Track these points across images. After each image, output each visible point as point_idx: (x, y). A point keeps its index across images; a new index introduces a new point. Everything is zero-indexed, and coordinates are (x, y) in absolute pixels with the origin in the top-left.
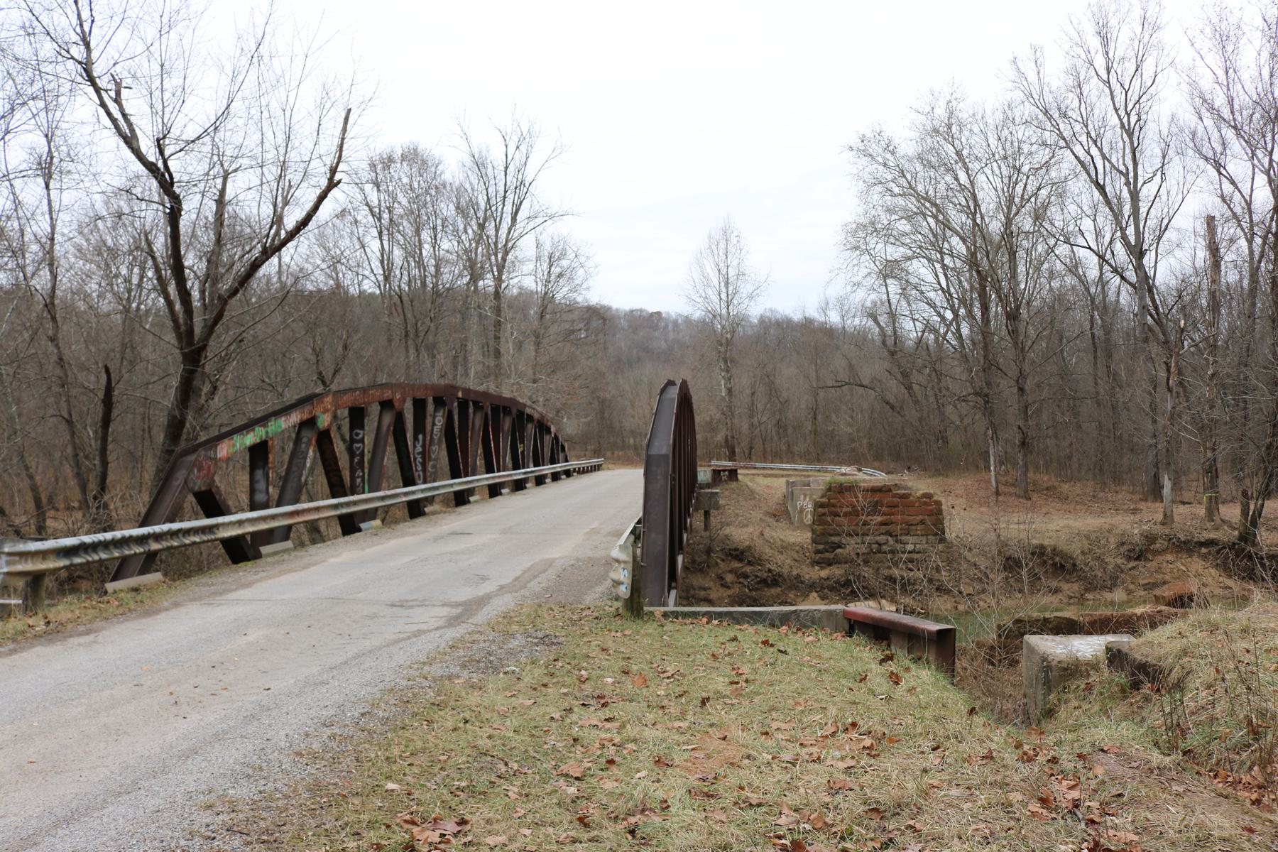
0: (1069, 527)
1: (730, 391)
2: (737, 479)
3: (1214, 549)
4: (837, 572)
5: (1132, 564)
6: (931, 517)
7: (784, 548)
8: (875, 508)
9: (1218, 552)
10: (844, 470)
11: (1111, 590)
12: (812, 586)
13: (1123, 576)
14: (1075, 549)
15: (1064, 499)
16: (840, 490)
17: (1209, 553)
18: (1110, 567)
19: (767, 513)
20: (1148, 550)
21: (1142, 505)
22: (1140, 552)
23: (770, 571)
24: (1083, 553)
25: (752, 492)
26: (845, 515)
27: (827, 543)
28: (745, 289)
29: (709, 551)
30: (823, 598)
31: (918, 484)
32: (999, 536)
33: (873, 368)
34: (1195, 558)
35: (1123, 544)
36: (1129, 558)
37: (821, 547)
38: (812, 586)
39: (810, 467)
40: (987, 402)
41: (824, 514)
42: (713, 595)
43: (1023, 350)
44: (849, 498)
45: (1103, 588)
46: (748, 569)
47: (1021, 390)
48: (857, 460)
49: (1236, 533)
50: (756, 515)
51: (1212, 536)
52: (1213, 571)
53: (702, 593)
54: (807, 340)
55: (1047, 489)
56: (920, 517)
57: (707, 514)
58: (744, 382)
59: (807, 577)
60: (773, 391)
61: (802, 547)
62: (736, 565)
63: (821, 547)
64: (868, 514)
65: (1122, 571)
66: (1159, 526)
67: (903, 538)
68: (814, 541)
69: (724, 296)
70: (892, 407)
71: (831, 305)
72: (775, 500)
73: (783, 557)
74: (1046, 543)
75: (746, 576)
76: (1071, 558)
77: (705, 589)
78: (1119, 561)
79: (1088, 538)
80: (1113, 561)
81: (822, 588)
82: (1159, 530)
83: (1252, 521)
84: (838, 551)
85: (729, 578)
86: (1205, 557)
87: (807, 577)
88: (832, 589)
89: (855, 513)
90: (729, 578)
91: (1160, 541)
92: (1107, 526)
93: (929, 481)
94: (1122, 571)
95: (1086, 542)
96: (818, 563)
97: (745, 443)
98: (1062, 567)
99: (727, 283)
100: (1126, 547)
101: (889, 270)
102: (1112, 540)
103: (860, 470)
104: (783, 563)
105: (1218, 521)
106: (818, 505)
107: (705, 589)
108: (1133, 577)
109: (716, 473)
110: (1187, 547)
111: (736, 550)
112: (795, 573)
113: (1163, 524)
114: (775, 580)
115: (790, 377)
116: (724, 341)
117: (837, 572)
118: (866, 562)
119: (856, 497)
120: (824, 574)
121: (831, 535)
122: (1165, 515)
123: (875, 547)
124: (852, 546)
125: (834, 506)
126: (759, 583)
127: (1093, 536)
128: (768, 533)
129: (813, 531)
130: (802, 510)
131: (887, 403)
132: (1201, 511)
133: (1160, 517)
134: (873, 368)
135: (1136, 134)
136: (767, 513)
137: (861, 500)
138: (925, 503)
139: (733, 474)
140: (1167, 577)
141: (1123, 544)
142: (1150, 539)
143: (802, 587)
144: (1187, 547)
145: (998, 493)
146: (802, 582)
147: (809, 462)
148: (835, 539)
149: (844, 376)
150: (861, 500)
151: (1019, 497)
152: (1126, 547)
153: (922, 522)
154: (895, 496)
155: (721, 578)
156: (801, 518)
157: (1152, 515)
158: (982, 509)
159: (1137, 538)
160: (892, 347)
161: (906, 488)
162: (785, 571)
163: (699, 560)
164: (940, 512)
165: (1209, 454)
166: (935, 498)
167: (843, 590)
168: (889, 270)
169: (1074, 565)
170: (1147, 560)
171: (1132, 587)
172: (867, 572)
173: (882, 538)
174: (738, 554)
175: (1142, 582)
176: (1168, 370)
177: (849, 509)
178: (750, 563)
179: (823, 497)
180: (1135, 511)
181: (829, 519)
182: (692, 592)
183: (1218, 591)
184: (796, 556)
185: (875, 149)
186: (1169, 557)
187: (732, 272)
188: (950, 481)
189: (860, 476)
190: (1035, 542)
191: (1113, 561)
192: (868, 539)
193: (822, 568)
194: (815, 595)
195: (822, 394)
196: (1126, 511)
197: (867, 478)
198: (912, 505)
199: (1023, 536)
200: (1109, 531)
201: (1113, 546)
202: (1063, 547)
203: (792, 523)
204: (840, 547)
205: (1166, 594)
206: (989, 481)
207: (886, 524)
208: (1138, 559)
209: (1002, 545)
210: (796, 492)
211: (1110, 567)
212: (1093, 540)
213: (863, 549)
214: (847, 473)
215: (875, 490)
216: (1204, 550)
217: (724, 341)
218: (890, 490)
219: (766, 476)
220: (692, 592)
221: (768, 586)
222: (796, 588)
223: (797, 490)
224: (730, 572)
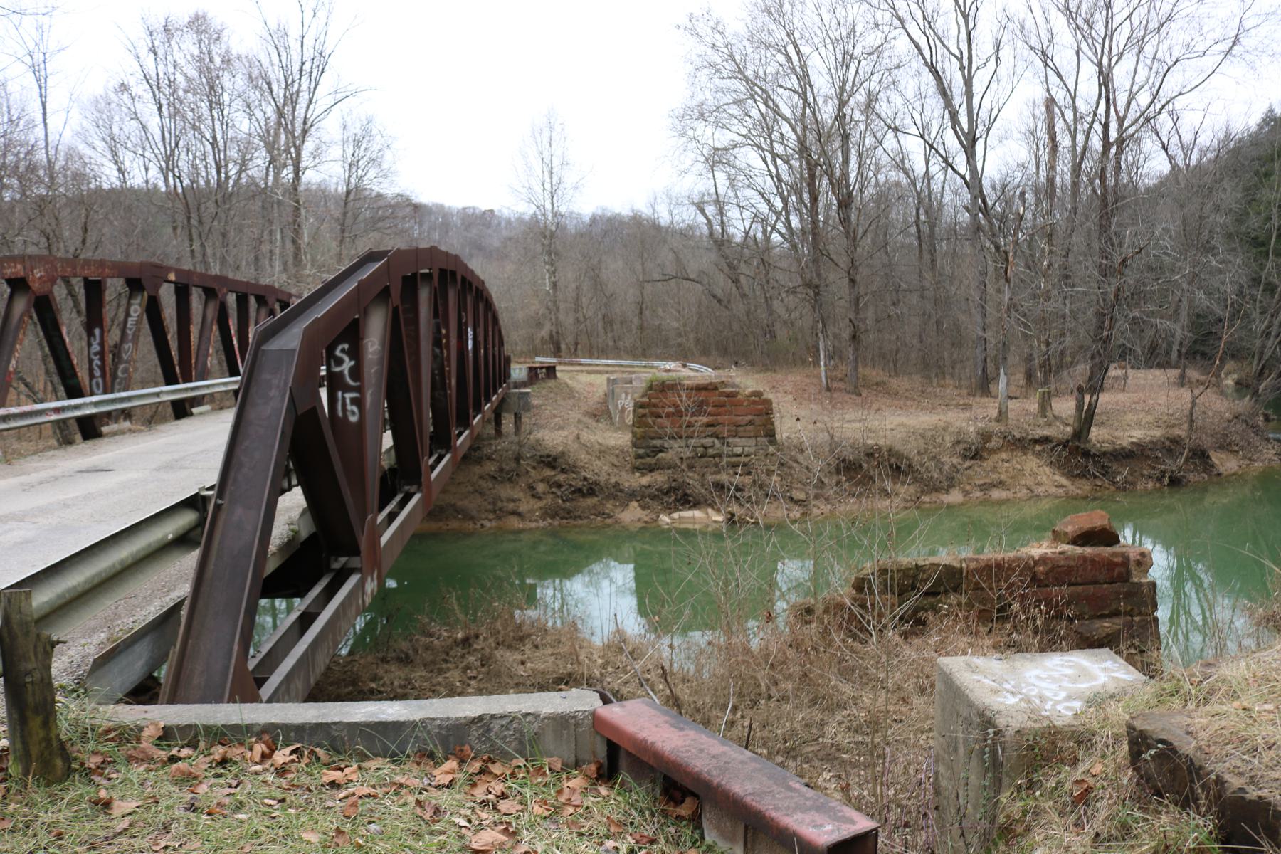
0: (902, 425)
1: (554, 285)
2: (555, 377)
3: (1050, 446)
4: (659, 478)
5: (968, 464)
6: (761, 416)
7: (603, 452)
8: (700, 408)
9: (1052, 449)
10: (670, 365)
11: (947, 492)
12: (632, 495)
13: (959, 476)
14: (911, 449)
15: (894, 394)
16: (662, 388)
17: (1044, 450)
18: (946, 467)
19: (586, 413)
20: (984, 449)
21: (970, 400)
22: (976, 453)
23: (585, 479)
24: (919, 453)
25: (571, 390)
26: (668, 415)
27: (648, 447)
28: (569, 178)
29: (517, 459)
30: (644, 508)
31: (746, 381)
32: (832, 437)
33: (702, 262)
34: (1030, 456)
35: (959, 442)
36: (965, 458)
38: (632, 495)
40: (817, 294)
41: (644, 416)
42: (523, 508)
43: (854, 239)
44: (672, 397)
45: (937, 490)
46: (561, 478)
47: (852, 281)
48: (684, 356)
49: (1069, 429)
50: (575, 415)
51: (1046, 432)
52: (1047, 469)
53: (511, 506)
54: (636, 236)
55: (877, 384)
56: (749, 417)
57: (517, 418)
58: (568, 276)
59: (626, 485)
60: (598, 285)
61: (622, 451)
62: (548, 472)
63: (641, 451)
64: (693, 415)
65: (958, 471)
66: (993, 423)
67: (730, 440)
68: (634, 445)
69: (548, 186)
70: (719, 301)
71: (659, 200)
72: (596, 398)
73: (599, 463)
74: (881, 442)
75: (559, 486)
76: (908, 459)
77: (514, 501)
78: (955, 460)
79: (923, 436)
80: (949, 460)
81: (643, 497)
82: (995, 427)
83: (1087, 418)
84: (660, 455)
85: (541, 488)
86: (1039, 455)
87: (626, 485)
88: (653, 498)
89: (679, 414)
90: (541, 488)
91: (995, 438)
92: (942, 424)
93: (756, 376)
94: (958, 471)
95: (921, 441)
96: (638, 469)
97: (570, 339)
98: (898, 468)
99: (551, 173)
100: (962, 446)
101: (717, 158)
102: (948, 438)
103: (685, 366)
104: (600, 470)
105: (1051, 418)
106: (639, 406)
107: (514, 501)
108: (969, 478)
109: (533, 371)
110: (1021, 444)
111: (548, 456)
112: (613, 480)
113: (998, 420)
114: (591, 489)
115: (616, 270)
116: (548, 233)
117: (659, 478)
118: (691, 467)
119: (679, 396)
120: (645, 480)
121: (653, 438)
122: (1000, 411)
123: (700, 450)
124: (675, 450)
126: (573, 492)
127: (929, 434)
128: (585, 436)
129: (634, 434)
130: (623, 410)
131: (714, 297)
132: (1033, 406)
133: (995, 414)
134: (702, 262)
135: (972, 14)
136: (586, 413)
137: (684, 400)
138: (754, 402)
139: (551, 371)
140: (1003, 477)
141: (959, 442)
142: (986, 436)
143: (621, 495)
144: (1021, 444)
146: (621, 491)
147: (635, 357)
148: (657, 443)
149: (670, 269)
150: (684, 400)
151: (849, 392)
152: (962, 446)
153: (750, 423)
154: (722, 394)
155: (532, 488)
156: (622, 418)
157: (987, 409)
158: (812, 406)
159: (973, 436)
160: (720, 242)
161: (734, 385)
162: (602, 479)
163: (508, 468)
165: (1044, 348)
166: (765, 397)
167: (666, 499)
168: (717, 158)
169: (910, 466)
170: (982, 458)
171: (968, 488)
172: (692, 479)
173: (708, 441)
174: (550, 461)
175: (978, 482)
176: (1007, 260)
177: (672, 410)
178: (563, 471)
179: (643, 396)
180: (967, 407)
181: (650, 421)
182: (499, 504)
183: (1053, 490)
184: (615, 461)
185: (703, 29)
186: (1004, 455)
187: (556, 162)
188: (779, 376)
189: (686, 372)
190: (870, 442)
191: (949, 460)
192: (692, 442)
193: (643, 475)
194: (635, 504)
195: (648, 287)
196: (958, 405)
197: (692, 374)
198: (740, 404)
199: (858, 435)
200: (945, 429)
201: (949, 445)
202: (899, 447)
203: (612, 424)
204: (661, 451)
205: (1070, 529)
206: (819, 377)
208: (973, 458)
209: (834, 444)
210: (617, 390)
211: (946, 467)
212: (929, 438)
213: (688, 453)
214: (669, 369)
215: (700, 388)
216: (1038, 448)
217: (548, 233)
219: (589, 372)
220: (499, 504)
221: (583, 496)
222: (615, 497)
224: (542, 481)
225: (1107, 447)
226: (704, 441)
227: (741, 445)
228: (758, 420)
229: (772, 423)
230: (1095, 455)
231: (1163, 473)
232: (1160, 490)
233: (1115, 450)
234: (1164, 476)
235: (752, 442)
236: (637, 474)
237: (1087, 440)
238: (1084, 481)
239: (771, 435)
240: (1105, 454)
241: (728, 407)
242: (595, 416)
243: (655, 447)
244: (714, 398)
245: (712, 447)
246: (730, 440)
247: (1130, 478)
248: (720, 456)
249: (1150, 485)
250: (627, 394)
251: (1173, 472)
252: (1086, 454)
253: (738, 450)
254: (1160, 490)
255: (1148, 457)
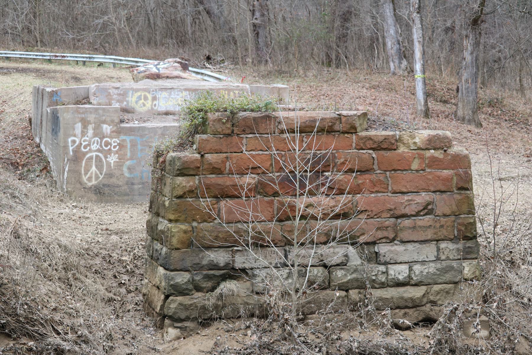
16: (238, 125)
27: (198, 267)
37: (182, 278)
39: (32, 54)
41: (191, 192)
55: (491, 104)
56: (424, 197)
61: (108, 259)
63: (182, 278)
67: (383, 249)
84: (228, 286)
96: (175, 319)
121: (209, 248)
123: (319, 273)
125: (217, 170)
130: (78, 157)
138: (434, 163)
145: (427, 114)
147: (28, 46)
148: (220, 257)
153: (427, 209)
156: (75, 173)
164: (465, 186)
166: (457, 149)
173: (335, 253)
179: (181, 146)
193: (186, 333)
198: (401, 167)
203: (54, 183)
207: (345, 215)
218: (352, 130)
223: (67, 114)
226: (324, 250)
227: (410, 260)
228: (444, 204)
229: (471, 211)
235: (429, 251)
236: (172, 332)
239: (468, 235)
241: (377, 175)
242: (15, 165)
243: (214, 266)
244: (348, 152)
245: (341, 265)
246: (383, 249)
248: (361, 286)
250: (85, 124)
253: (399, 272)
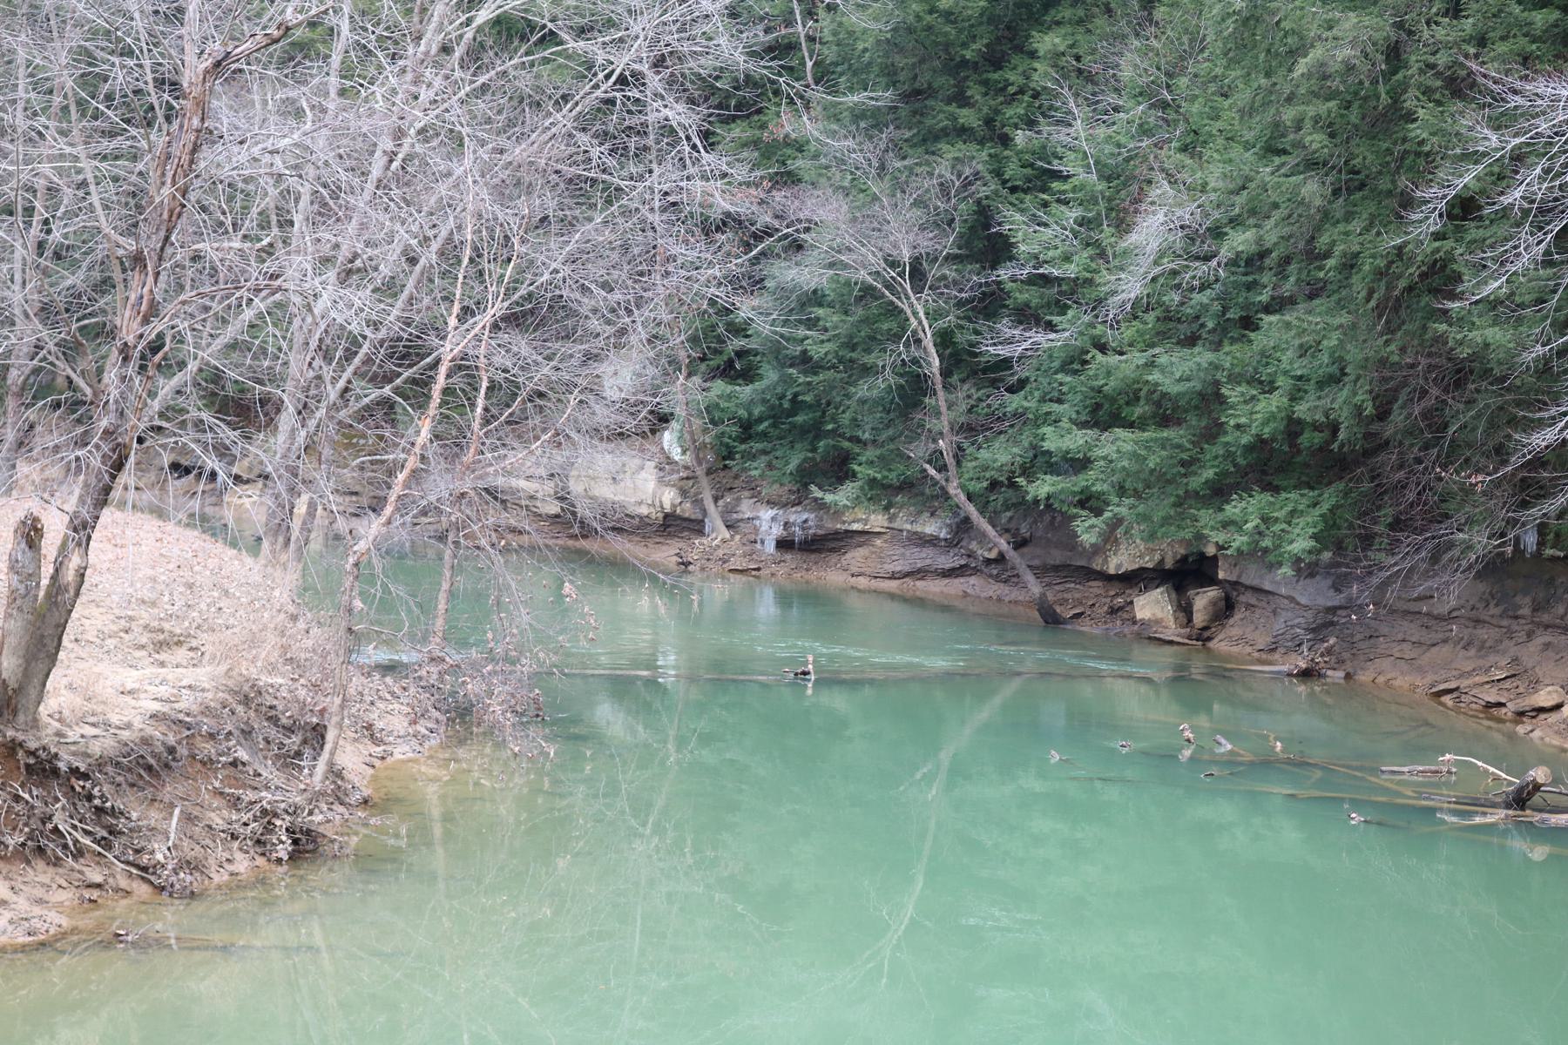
225: (103, 745)
230: (75, 771)
231: (268, 814)
232: (262, 881)
233: (126, 749)
234: (269, 828)
237: (35, 723)
238: (41, 873)
240: (101, 764)
247: (191, 851)
249: (242, 864)
251: (295, 811)
252: (43, 769)
254: (262, 881)
255: (208, 763)
